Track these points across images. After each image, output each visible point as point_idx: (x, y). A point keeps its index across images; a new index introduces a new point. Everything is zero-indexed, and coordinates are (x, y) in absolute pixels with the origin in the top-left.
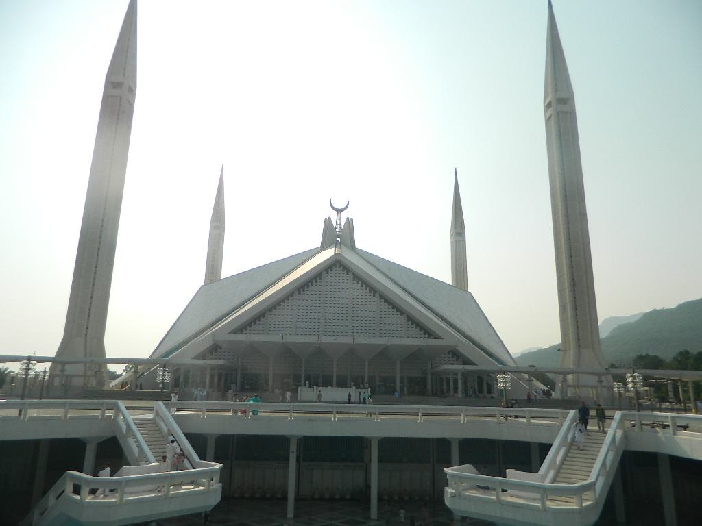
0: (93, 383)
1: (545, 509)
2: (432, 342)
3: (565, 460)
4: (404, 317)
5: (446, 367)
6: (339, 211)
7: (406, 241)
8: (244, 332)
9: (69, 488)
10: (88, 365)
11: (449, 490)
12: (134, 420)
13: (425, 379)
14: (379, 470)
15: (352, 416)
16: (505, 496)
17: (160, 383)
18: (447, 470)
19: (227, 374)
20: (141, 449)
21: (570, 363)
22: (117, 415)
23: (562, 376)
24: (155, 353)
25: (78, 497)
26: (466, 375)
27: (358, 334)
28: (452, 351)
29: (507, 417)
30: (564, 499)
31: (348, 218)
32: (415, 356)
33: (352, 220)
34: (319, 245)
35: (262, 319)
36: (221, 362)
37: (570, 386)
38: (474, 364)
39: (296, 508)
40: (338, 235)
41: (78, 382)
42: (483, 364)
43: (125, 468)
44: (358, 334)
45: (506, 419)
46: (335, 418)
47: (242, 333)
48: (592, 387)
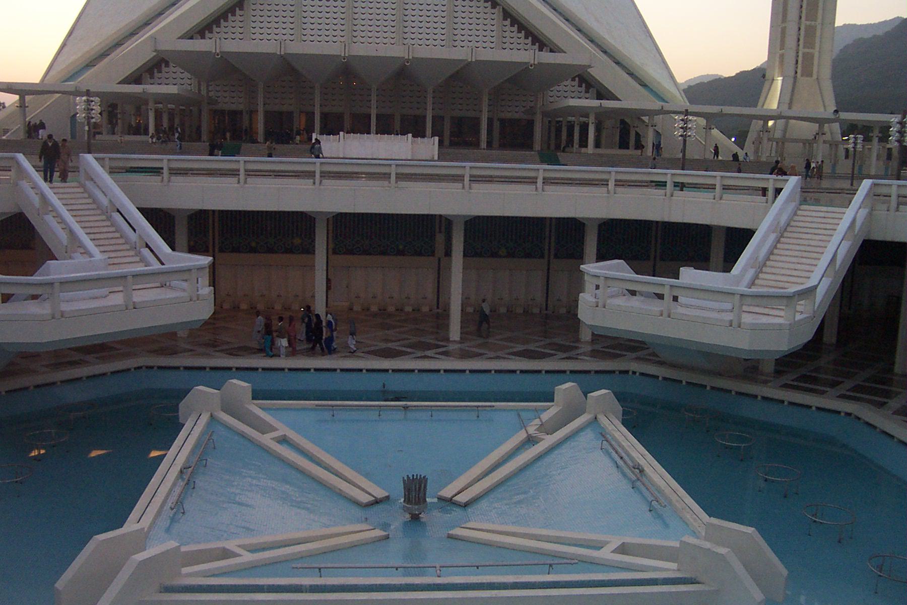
2: (546, 57)
3: (772, 253)
8: (208, 35)
13: (531, 123)
14: (465, 268)
20: (71, 233)
23: (761, 122)
24: (51, 74)
26: (602, 117)
28: (579, 76)
30: (766, 311)
32: (519, 81)
35: (238, 12)
36: (172, 90)
42: (630, 99)
47: (203, 37)
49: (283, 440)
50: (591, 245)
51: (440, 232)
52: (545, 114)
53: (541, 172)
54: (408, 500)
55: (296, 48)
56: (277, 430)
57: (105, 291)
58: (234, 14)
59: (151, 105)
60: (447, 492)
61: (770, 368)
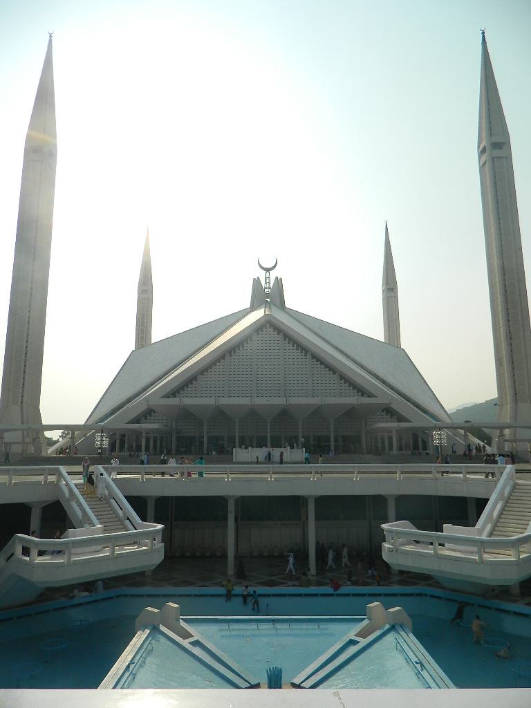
0: (32, 449)
1: (483, 562)
3: (502, 514)
4: (336, 377)
6: (268, 270)
7: (336, 298)
9: (19, 550)
11: (386, 545)
12: (76, 485)
14: (317, 528)
16: (440, 549)
17: (99, 448)
18: (383, 526)
19: (162, 437)
21: (507, 418)
22: (59, 480)
23: (498, 431)
24: (90, 420)
25: (28, 559)
26: (400, 432)
27: (290, 395)
28: (385, 409)
33: (281, 279)
35: (194, 382)
36: (156, 426)
37: (506, 441)
38: (407, 421)
40: (268, 295)
41: (16, 449)
42: (418, 421)
44: (290, 395)
46: (271, 478)
49: (197, 643)
53: (356, 468)
55: (225, 401)
56: (192, 636)
57: (100, 547)
58: (191, 384)
59: (144, 435)
60: (297, 681)
61: (517, 591)
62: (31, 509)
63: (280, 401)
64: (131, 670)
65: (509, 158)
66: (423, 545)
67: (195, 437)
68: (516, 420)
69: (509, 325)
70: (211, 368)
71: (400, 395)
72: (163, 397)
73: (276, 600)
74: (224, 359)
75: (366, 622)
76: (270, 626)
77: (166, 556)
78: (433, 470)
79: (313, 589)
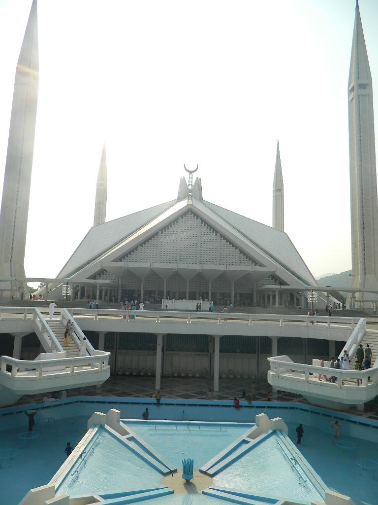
0: (18, 295)
2: (258, 268)
5: (268, 286)
6: (191, 172)
7: (239, 196)
9: (4, 367)
10: (13, 282)
11: (271, 373)
12: (47, 321)
13: (252, 295)
15: (200, 320)
20: (53, 342)
22: (35, 318)
23: (351, 294)
24: (60, 275)
25: (10, 374)
26: (281, 292)
28: (271, 275)
29: (313, 322)
31: (198, 178)
32: (247, 278)
34: (176, 197)
36: (107, 282)
37: (356, 301)
38: (287, 284)
39: (162, 382)
42: (293, 284)
43: (42, 354)
45: (313, 324)
47: (121, 261)
48: (373, 302)
49: (132, 439)
50: (275, 348)
51: (211, 342)
52: (258, 291)
54: (184, 472)
58: (134, 252)
59: (98, 287)
60: (204, 469)
61: (363, 407)
62: (13, 338)
63: (197, 267)
64: (83, 457)
65: (370, 96)
66: (297, 373)
67: (134, 291)
68: (364, 286)
69: (363, 218)
70: (148, 242)
71: (282, 266)
72: (113, 261)
73: (190, 408)
74: (157, 235)
75: (255, 427)
76: (185, 428)
77: (111, 375)
78: (328, 321)
79: (216, 402)
